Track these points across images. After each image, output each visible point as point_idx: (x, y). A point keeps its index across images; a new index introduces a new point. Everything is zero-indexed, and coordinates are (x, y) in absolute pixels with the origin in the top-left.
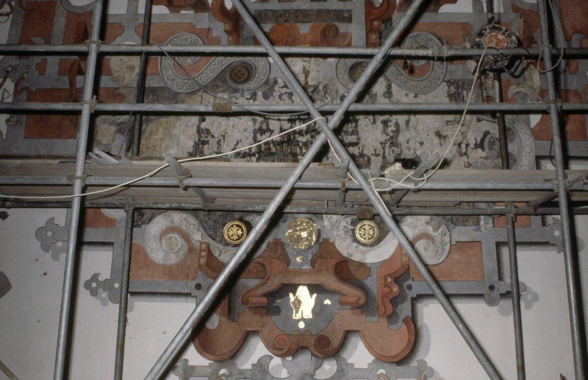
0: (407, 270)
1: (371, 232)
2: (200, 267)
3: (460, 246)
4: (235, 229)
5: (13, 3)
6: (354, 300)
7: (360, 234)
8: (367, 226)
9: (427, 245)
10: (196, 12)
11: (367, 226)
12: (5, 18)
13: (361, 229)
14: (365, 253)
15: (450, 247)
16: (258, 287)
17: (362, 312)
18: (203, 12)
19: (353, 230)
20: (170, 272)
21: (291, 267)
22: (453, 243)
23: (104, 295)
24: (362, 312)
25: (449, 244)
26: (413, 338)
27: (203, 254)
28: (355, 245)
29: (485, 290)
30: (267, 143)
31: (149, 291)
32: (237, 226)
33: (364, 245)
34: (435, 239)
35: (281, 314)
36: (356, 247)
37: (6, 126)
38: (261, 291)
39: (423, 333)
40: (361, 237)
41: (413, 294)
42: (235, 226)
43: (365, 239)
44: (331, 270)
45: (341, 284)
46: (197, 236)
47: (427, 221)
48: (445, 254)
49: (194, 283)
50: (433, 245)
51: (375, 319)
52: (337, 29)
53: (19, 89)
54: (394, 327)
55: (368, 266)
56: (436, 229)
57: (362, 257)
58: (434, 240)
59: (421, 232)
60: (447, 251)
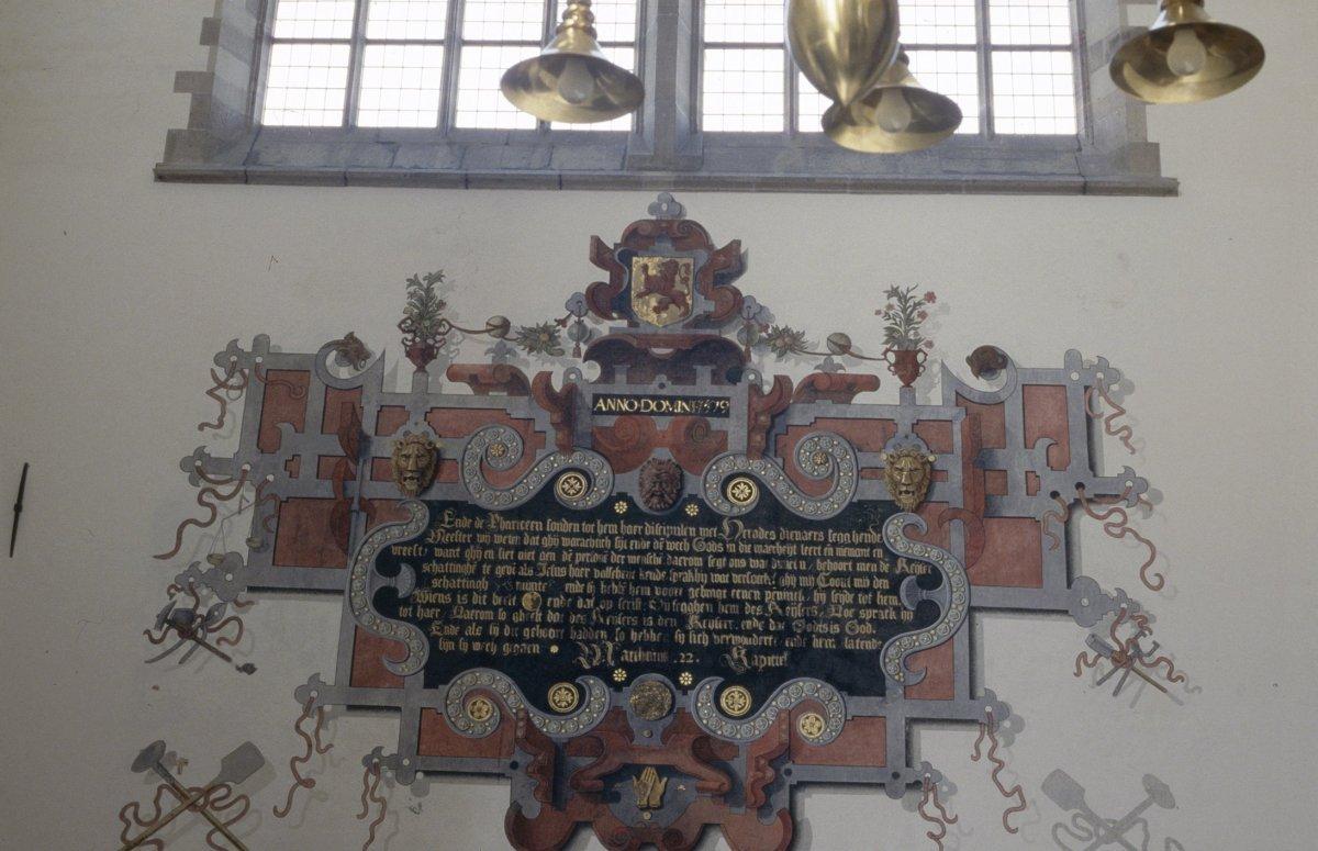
1: (742, 701)
2: (516, 739)
3: (855, 721)
4: (563, 692)
5: (247, 371)
6: (716, 785)
10: (510, 394)
12: (239, 392)
16: (592, 767)
17: (725, 802)
18: (521, 395)
20: (479, 746)
21: (634, 743)
22: (849, 718)
23: (389, 774)
24: (725, 802)
26: (790, 837)
27: (521, 724)
29: (887, 779)
30: (608, 582)
31: (449, 769)
32: (566, 689)
35: (622, 802)
38: (595, 772)
39: (803, 832)
41: (793, 780)
42: (563, 690)
44: (687, 750)
45: (699, 766)
46: (515, 699)
49: (509, 762)
51: (742, 810)
52: (708, 425)
54: (765, 821)
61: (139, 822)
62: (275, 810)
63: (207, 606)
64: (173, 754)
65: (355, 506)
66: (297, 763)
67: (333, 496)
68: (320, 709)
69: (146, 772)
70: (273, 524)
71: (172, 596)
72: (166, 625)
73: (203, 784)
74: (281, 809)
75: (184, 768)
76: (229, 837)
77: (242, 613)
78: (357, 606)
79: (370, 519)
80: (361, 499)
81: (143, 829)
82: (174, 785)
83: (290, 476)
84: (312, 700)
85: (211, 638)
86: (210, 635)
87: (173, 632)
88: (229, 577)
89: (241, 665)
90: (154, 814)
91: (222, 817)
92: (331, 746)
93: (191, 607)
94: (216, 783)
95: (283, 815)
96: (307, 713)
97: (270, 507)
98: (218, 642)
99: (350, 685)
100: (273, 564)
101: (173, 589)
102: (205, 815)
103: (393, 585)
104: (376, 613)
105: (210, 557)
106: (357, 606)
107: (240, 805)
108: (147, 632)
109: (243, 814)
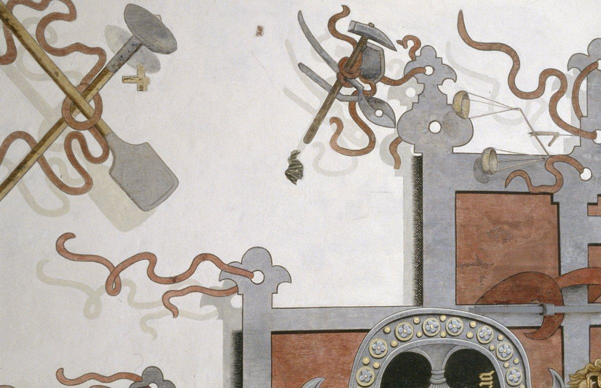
37: (481, 151)
53: (560, 166)
61: (44, 23)
62: (69, 236)
63: (389, 98)
64: (156, 67)
65: (552, 309)
66: (145, 263)
67: (563, 273)
68: (235, 290)
69: (124, 26)
70: (518, 185)
71: (403, 43)
72: (357, 38)
73: (108, 118)
74: (69, 245)
75: (134, 86)
76: (22, 167)
77: (382, 153)
78: (399, 328)
79: (533, 332)
80: (562, 315)
81: (32, 30)
82: (105, 72)
83: (589, 204)
84: (250, 275)
85: (340, 109)
86: (345, 106)
87: (347, 49)
88: (435, 127)
89: (299, 158)
90: (59, 45)
91: (55, 154)
92: (175, 312)
93: (390, 73)
94: (109, 138)
95: (61, 250)
96: (228, 269)
97: (542, 178)
98: (335, 120)
99: (273, 333)
100: (457, 192)
101: (414, 44)
102: (59, 124)
103: (432, 380)
104: (389, 359)
105: (465, 95)
106: (399, 328)
107: (74, 178)
108: (346, 11)
109: (62, 186)
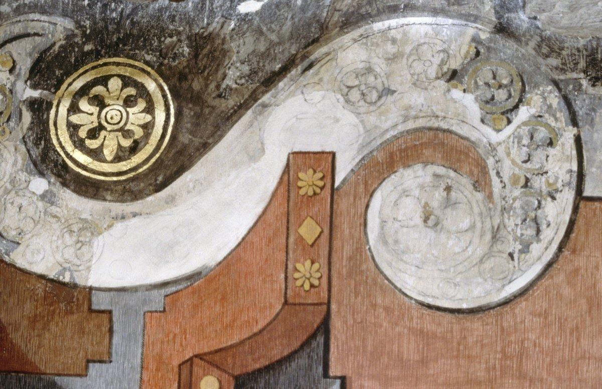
0: (313, 336)
7: (73, 128)
8: (115, 84)
9: (439, 195)
11: (115, 84)
13: (84, 105)
14: (90, 229)
15: (576, 209)
19: (39, 108)
25: (568, 197)
28: (39, 185)
33: (88, 188)
34: (490, 162)
36: (43, 197)
40: (80, 144)
43: (96, 154)
47: (455, 64)
48: (542, 252)
50: (479, 196)
55: (100, 302)
56: (500, 112)
57: (69, 253)
58: (484, 170)
59: (411, 125)
60: (553, 235)
